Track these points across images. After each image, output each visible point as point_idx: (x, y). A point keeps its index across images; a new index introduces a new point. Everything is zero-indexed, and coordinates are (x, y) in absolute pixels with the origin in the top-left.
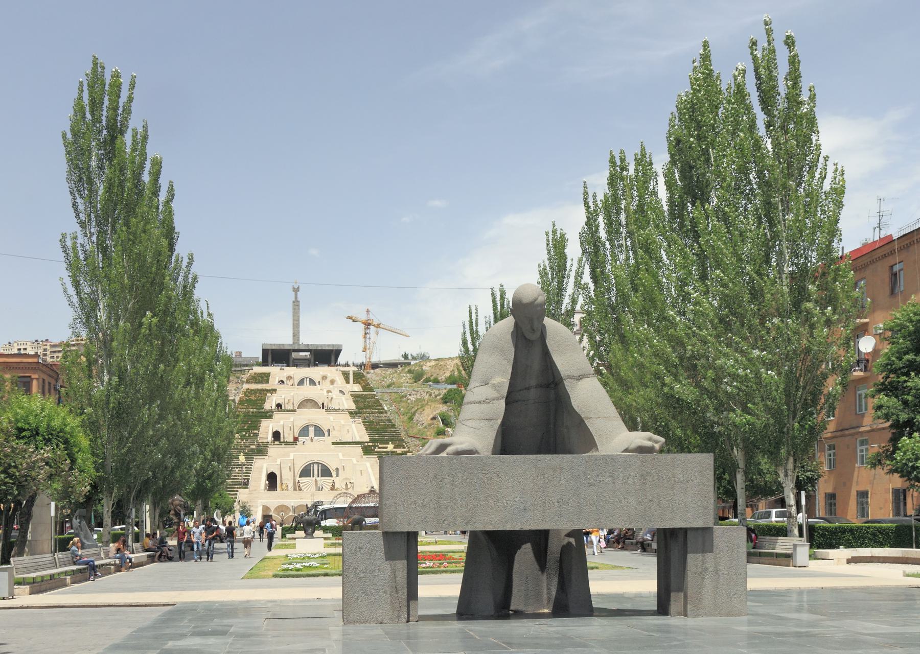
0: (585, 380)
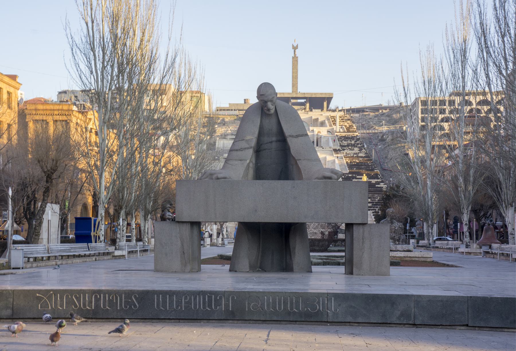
0: (300, 138)
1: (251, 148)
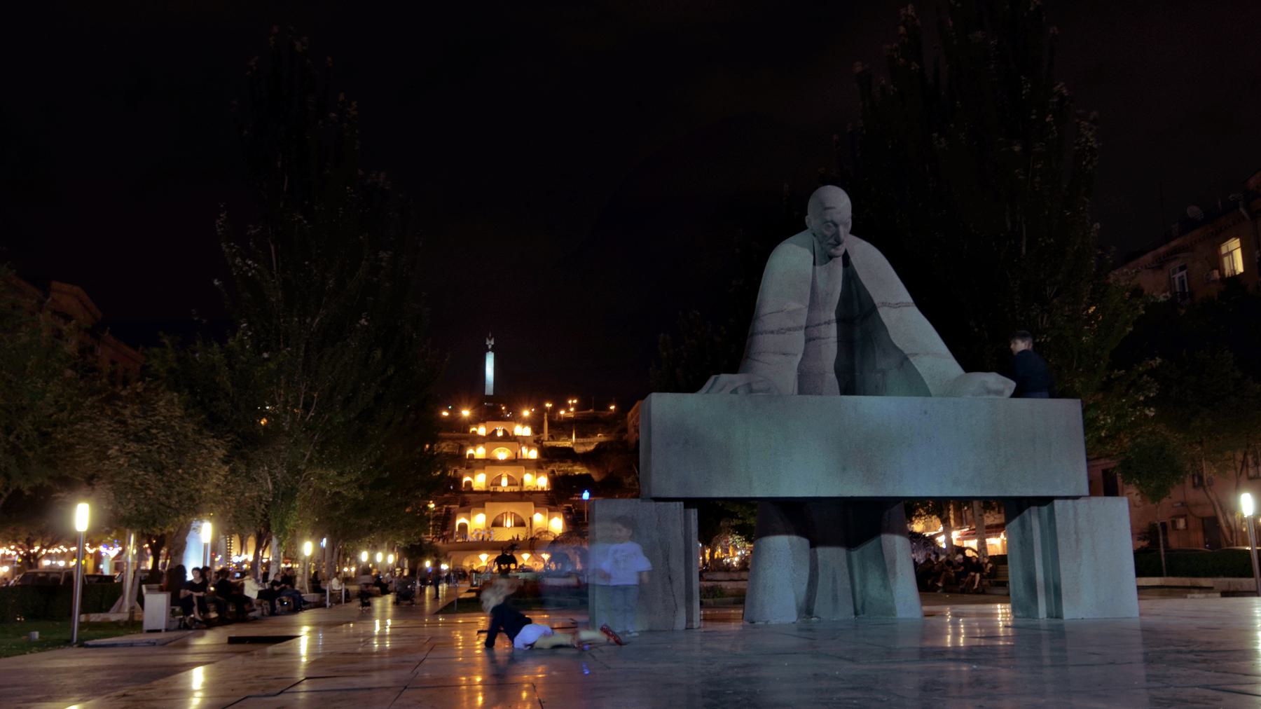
1: (801, 328)
